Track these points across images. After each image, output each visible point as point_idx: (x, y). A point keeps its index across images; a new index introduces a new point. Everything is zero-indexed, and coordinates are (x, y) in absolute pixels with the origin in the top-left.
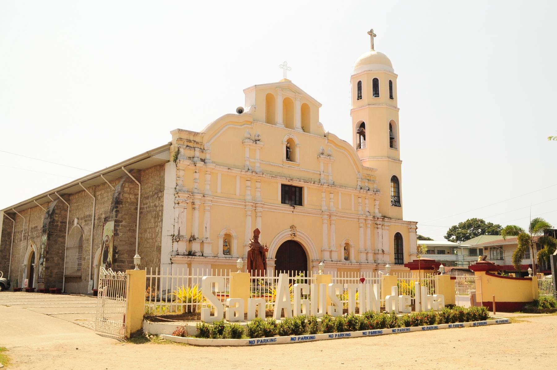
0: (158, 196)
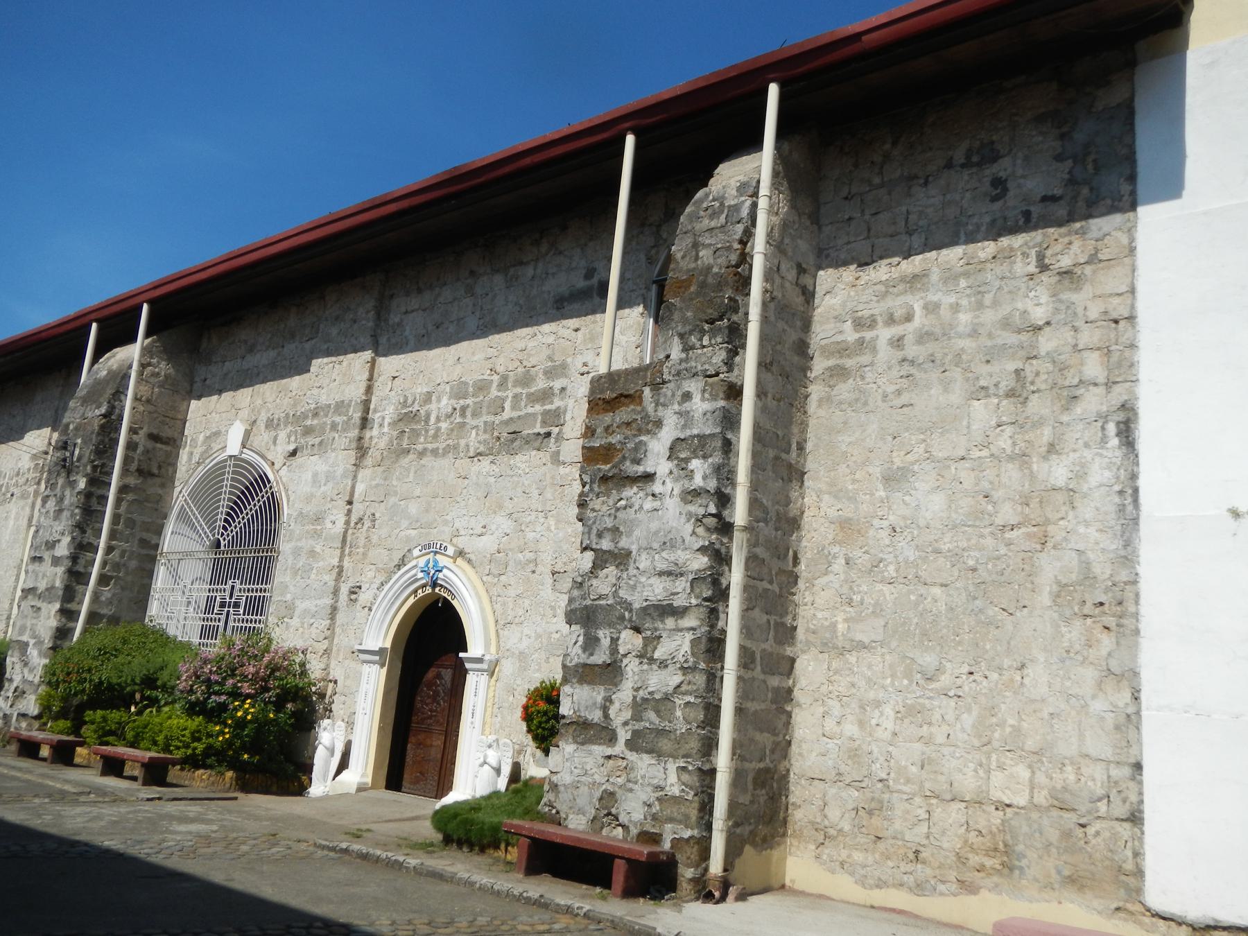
0: (1043, 267)
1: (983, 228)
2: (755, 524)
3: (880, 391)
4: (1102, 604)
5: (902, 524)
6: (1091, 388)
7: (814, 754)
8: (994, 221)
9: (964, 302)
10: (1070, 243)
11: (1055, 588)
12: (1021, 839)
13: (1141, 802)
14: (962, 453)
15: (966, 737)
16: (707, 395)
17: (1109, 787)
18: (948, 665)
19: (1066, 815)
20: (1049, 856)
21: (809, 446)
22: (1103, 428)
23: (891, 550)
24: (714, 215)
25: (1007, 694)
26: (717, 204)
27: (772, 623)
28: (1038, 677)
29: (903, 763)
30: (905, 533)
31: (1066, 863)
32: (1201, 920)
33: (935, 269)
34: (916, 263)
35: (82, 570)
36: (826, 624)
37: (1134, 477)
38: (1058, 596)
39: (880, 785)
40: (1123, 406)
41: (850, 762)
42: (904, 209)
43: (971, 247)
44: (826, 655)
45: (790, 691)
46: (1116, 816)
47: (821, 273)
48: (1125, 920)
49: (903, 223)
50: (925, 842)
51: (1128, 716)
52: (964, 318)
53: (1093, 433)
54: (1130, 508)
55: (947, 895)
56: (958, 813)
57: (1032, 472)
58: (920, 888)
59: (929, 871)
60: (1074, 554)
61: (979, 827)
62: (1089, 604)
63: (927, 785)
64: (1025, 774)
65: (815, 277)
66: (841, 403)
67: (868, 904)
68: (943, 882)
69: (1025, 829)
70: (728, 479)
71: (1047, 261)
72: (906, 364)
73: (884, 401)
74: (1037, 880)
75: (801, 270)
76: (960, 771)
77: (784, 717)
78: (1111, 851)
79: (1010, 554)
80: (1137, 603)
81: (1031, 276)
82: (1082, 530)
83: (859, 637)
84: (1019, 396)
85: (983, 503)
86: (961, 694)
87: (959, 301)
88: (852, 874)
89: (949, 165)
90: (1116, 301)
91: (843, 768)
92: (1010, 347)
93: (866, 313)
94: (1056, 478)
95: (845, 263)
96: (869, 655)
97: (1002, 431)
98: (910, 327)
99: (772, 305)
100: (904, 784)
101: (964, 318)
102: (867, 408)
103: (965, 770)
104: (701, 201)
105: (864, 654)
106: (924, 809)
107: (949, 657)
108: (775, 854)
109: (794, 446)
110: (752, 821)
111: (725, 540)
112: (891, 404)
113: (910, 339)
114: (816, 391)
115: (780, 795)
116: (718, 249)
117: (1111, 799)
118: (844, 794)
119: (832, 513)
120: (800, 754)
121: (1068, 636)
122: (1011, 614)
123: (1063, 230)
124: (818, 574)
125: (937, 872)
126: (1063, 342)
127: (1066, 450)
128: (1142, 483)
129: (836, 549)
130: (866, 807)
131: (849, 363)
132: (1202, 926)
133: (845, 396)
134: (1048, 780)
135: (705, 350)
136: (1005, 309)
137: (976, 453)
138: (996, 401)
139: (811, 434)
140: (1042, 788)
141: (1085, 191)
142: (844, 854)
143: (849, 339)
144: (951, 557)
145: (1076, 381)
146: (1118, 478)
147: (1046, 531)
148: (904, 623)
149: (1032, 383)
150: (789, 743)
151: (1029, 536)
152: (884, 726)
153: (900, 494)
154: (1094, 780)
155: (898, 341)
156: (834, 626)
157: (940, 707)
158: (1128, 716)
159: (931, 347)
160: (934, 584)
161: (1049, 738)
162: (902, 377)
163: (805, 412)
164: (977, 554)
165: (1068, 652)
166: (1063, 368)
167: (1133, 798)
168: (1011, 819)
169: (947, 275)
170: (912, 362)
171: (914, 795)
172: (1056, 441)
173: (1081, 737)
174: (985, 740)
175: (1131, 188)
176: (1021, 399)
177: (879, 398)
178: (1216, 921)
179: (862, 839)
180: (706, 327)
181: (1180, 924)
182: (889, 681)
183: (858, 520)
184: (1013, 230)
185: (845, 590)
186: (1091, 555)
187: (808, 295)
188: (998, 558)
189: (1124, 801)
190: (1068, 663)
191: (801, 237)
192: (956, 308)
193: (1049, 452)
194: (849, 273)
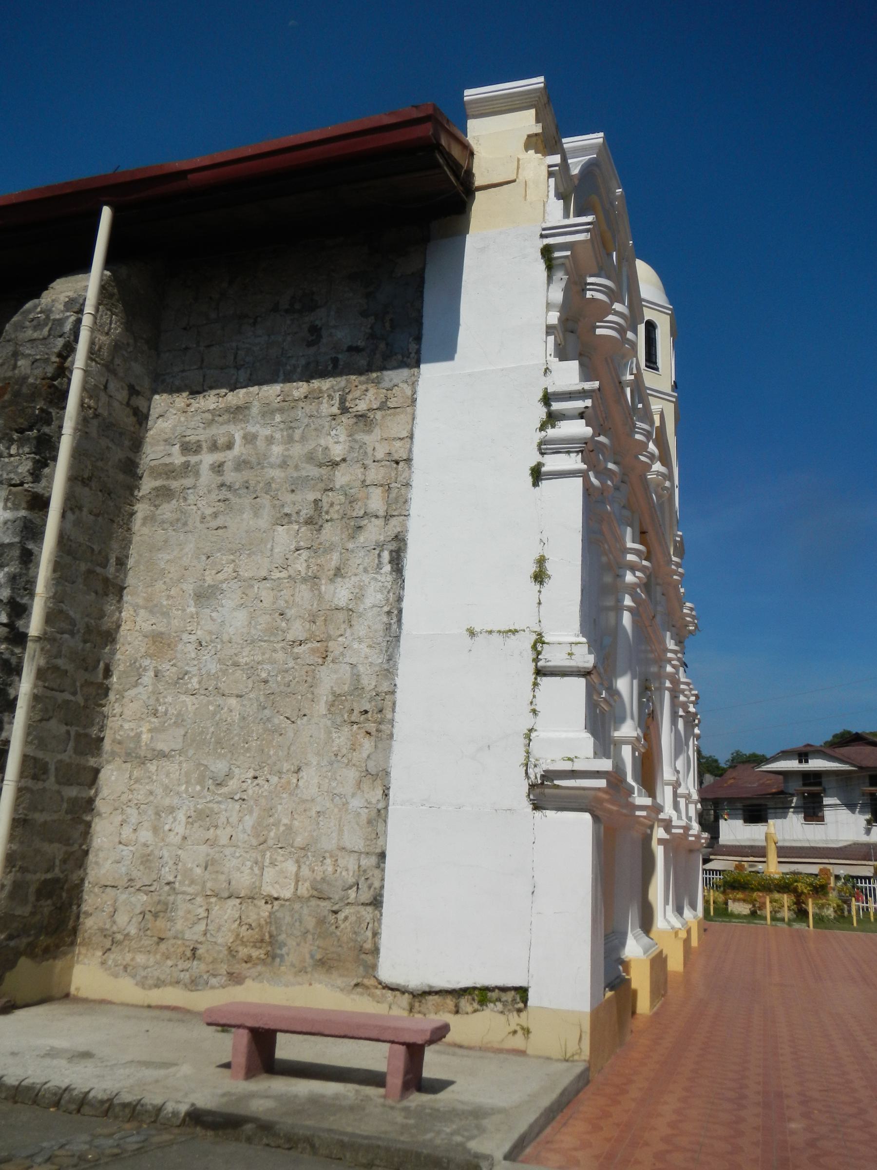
0: (344, 410)
1: (299, 370)
2: (59, 636)
3: (199, 512)
4: (366, 712)
5: (208, 638)
6: (373, 519)
7: (110, 862)
8: (308, 364)
9: (278, 435)
10: (367, 390)
11: (331, 698)
12: (284, 928)
13: (382, 887)
14: (264, 573)
15: (246, 838)
16: (9, 505)
17: (359, 876)
18: (237, 771)
19: (323, 904)
20: (306, 943)
21: (131, 562)
22: (379, 556)
23: (196, 663)
24: (38, 327)
25: (284, 795)
26: (42, 316)
27: (73, 733)
28: (310, 779)
29: (190, 865)
30: (210, 647)
31: (319, 947)
32: (419, 988)
33: (256, 403)
34: (239, 396)
36: (132, 734)
37: (400, 599)
38: (332, 705)
39: (167, 888)
40: (396, 536)
41: (142, 868)
42: (234, 344)
43: (288, 385)
44: (129, 765)
45: (91, 801)
46: (362, 901)
47: (157, 397)
48: (362, 994)
49: (232, 358)
50: (202, 939)
51: (379, 811)
52: (277, 450)
53: (370, 560)
54: (395, 627)
55: (218, 988)
56: (232, 910)
57: (320, 593)
58: (194, 984)
59: (203, 967)
60: (348, 668)
61: (250, 921)
62: (356, 712)
63: (209, 885)
64: (290, 867)
65: (150, 400)
66: (163, 522)
67: (146, 1004)
68: (215, 976)
69: (288, 919)
70: (26, 589)
71: (347, 404)
72: (224, 489)
73: (202, 522)
74: (293, 965)
75: (133, 391)
76: (238, 869)
77: (81, 828)
78: (355, 933)
79: (296, 667)
80: (394, 711)
81: (334, 417)
82: (356, 645)
83: (160, 746)
84: (316, 523)
85: (278, 620)
86: (245, 797)
87: (274, 434)
88: (134, 976)
89: (275, 309)
90: (398, 444)
91: (135, 874)
92: (312, 479)
93: (193, 439)
94: (339, 599)
95: (179, 390)
96: (168, 763)
97: (298, 554)
98: (230, 455)
99: (95, 422)
100: (189, 886)
101: (277, 450)
102: (186, 528)
103: (243, 868)
104: (29, 311)
105: (164, 762)
106: (204, 908)
107: (238, 763)
108: (59, 964)
109: (113, 561)
110: (32, 932)
111: (17, 650)
112: (207, 525)
113: (229, 466)
114: (142, 509)
115: (71, 905)
116: (36, 360)
117: (360, 886)
118: (133, 899)
119: (146, 627)
120: (97, 863)
121: (337, 741)
122: (293, 722)
123: (363, 378)
124: (127, 687)
125: (211, 967)
126: (354, 478)
127: (349, 574)
128: (405, 605)
129: (146, 662)
130: (153, 910)
131: (175, 484)
132: (420, 992)
133: (168, 515)
134: (311, 872)
135: (12, 459)
136: (310, 445)
137: (276, 575)
138: (297, 527)
139: (133, 551)
140: (306, 881)
141: (382, 346)
142: (128, 956)
143: (176, 462)
144: (248, 670)
145: (361, 513)
146: (388, 600)
147: (327, 647)
148: (202, 732)
149: (327, 513)
150: (87, 853)
151: (313, 651)
152: (176, 831)
153: (208, 611)
154: (347, 870)
155: (219, 466)
156: (138, 736)
157: (226, 810)
158: (379, 811)
159: (247, 474)
160: (231, 695)
161: (315, 834)
162: (219, 501)
163: (129, 529)
164: (269, 667)
165: (336, 755)
166: (352, 501)
167: (377, 884)
168: (277, 911)
169: (266, 409)
170: (230, 488)
171: (197, 895)
172: (342, 566)
173: (341, 831)
174: (262, 839)
175: (417, 347)
176: (317, 527)
177: (198, 519)
178: (430, 987)
179: (146, 942)
180: (15, 436)
181: (403, 993)
182: (183, 787)
183: (169, 634)
184: (323, 374)
185: (152, 701)
186: (361, 669)
187: (142, 418)
188: (287, 671)
189: (370, 887)
190: (335, 765)
192: (270, 440)
193: (335, 575)
194: (181, 400)
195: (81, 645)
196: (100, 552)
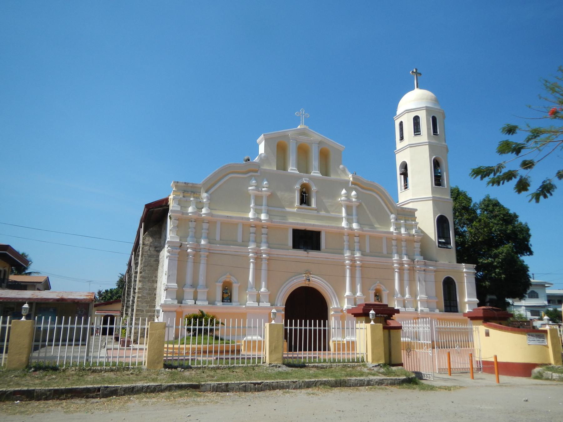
35: (128, 305)
77: (152, 319)
191: (156, 242)
195: (148, 292)
196: (151, 276)
